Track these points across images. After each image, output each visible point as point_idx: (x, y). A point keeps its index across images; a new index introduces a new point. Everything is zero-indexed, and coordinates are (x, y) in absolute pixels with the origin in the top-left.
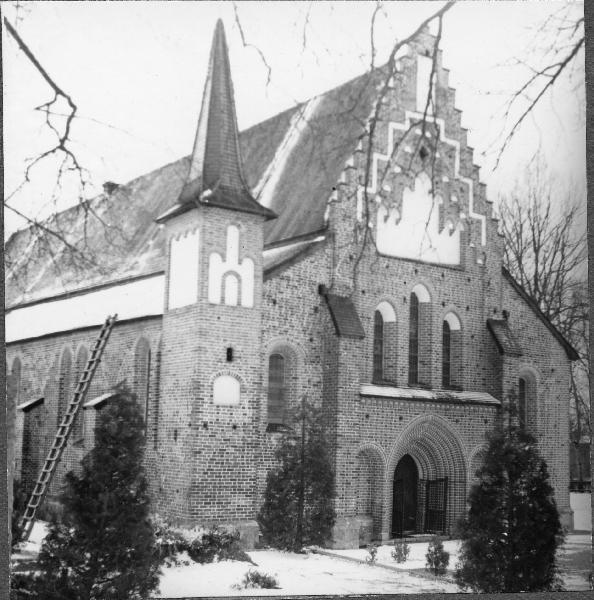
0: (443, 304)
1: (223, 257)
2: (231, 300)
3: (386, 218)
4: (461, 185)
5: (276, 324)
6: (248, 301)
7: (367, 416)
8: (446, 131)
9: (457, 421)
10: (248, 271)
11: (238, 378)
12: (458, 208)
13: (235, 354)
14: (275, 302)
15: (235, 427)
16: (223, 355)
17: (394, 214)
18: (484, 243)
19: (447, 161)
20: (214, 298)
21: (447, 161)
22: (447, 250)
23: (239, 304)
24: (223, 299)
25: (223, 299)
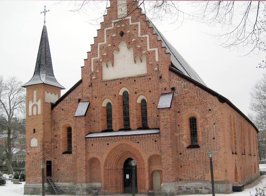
0: (136, 93)
1: (33, 102)
2: (35, 113)
3: (107, 66)
4: (142, 39)
5: (64, 117)
6: (40, 112)
7: (92, 145)
8: (132, 20)
9: (138, 143)
10: (39, 103)
11: (37, 138)
12: (141, 50)
13: (36, 131)
14: (63, 110)
15: (36, 154)
16: (33, 131)
17: (110, 64)
18: (157, 59)
19: (133, 32)
20: (30, 114)
21: (133, 32)
22: (140, 69)
23: (37, 115)
24: (32, 113)
25: (32, 113)
